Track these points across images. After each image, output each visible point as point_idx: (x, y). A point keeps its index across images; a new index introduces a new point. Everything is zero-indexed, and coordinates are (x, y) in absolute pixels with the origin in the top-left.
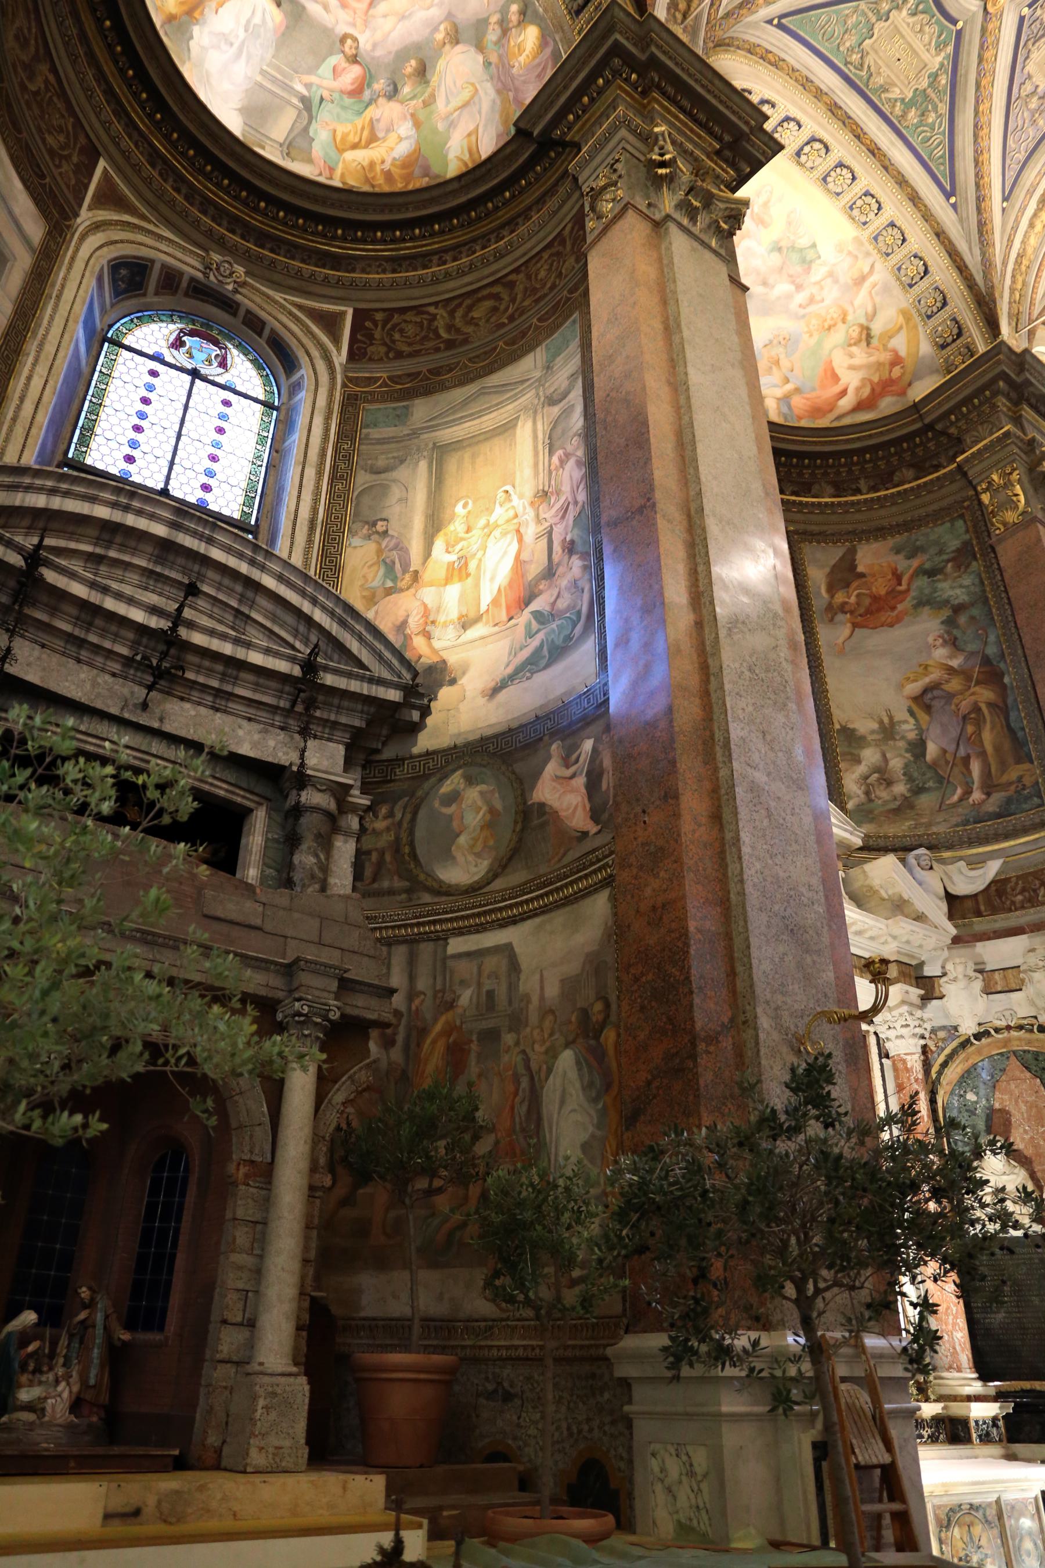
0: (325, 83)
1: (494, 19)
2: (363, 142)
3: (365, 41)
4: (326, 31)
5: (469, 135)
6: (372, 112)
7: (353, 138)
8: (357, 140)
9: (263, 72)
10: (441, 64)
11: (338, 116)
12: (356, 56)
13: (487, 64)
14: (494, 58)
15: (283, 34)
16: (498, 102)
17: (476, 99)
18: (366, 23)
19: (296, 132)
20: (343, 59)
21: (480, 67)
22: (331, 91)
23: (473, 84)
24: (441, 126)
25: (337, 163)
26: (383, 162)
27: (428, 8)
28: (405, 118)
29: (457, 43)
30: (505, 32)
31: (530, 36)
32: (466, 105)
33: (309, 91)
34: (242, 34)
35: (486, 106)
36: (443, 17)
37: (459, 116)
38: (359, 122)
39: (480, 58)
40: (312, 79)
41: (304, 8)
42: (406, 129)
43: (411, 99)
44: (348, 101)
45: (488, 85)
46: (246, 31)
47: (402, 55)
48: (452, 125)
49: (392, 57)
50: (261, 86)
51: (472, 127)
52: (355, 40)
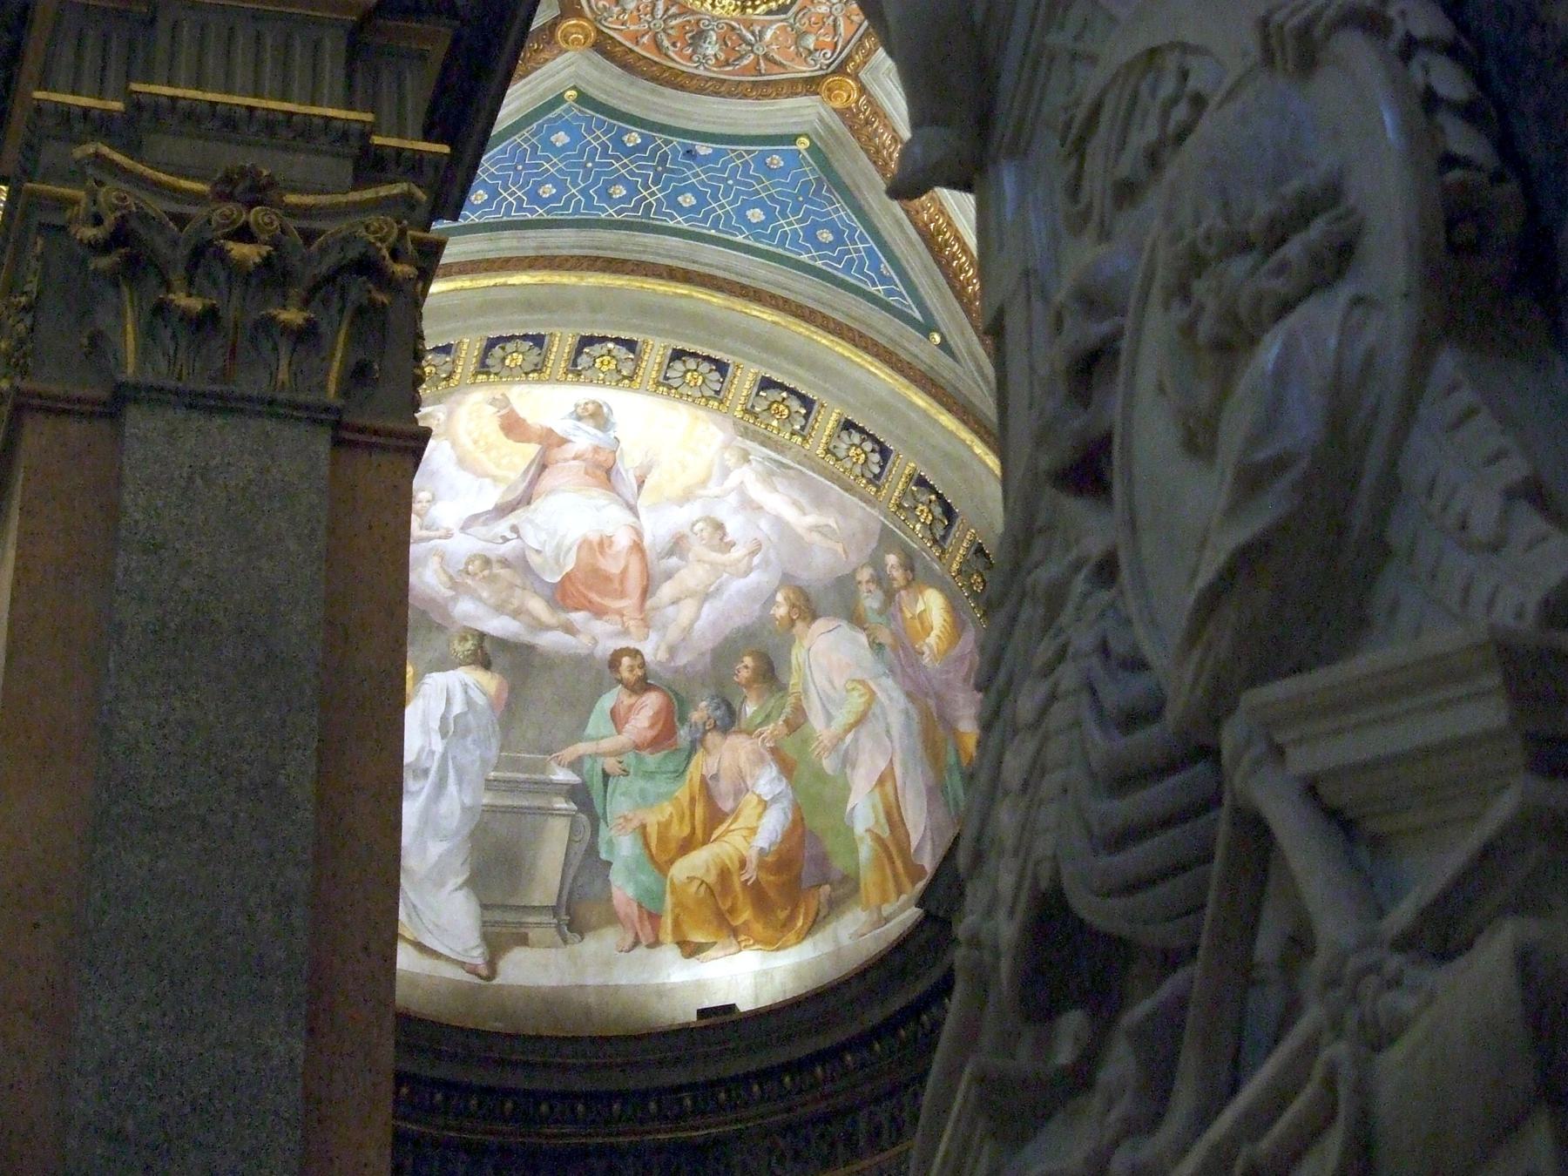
0: (606, 745)
1: (865, 574)
2: (699, 832)
3: (652, 648)
4: (581, 663)
5: (881, 781)
6: (702, 765)
7: (679, 831)
8: (686, 831)
9: (490, 785)
10: (797, 655)
11: (643, 794)
12: (644, 678)
13: (877, 647)
14: (885, 637)
15: (508, 705)
16: (914, 712)
17: (876, 709)
18: (646, 623)
19: (576, 862)
20: (624, 690)
21: (867, 655)
22: (617, 753)
23: (862, 682)
24: (828, 764)
25: (661, 898)
26: (743, 864)
27: (746, 574)
28: (762, 760)
29: (814, 617)
30: (890, 596)
31: (932, 605)
32: (860, 721)
33: (579, 773)
34: (438, 745)
35: (896, 721)
36: (777, 583)
37: (856, 740)
38: (683, 792)
39: (863, 638)
40: (582, 748)
41: (531, 648)
42: (767, 782)
43: (761, 724)
44: (652, 760)
45: (889, 682)
46: (443, 737)
47: (725, 652)
48: (848, 761)
49: (708, 658)
50: (492, 809)
51: (882, 765)
52: (635, 653)
